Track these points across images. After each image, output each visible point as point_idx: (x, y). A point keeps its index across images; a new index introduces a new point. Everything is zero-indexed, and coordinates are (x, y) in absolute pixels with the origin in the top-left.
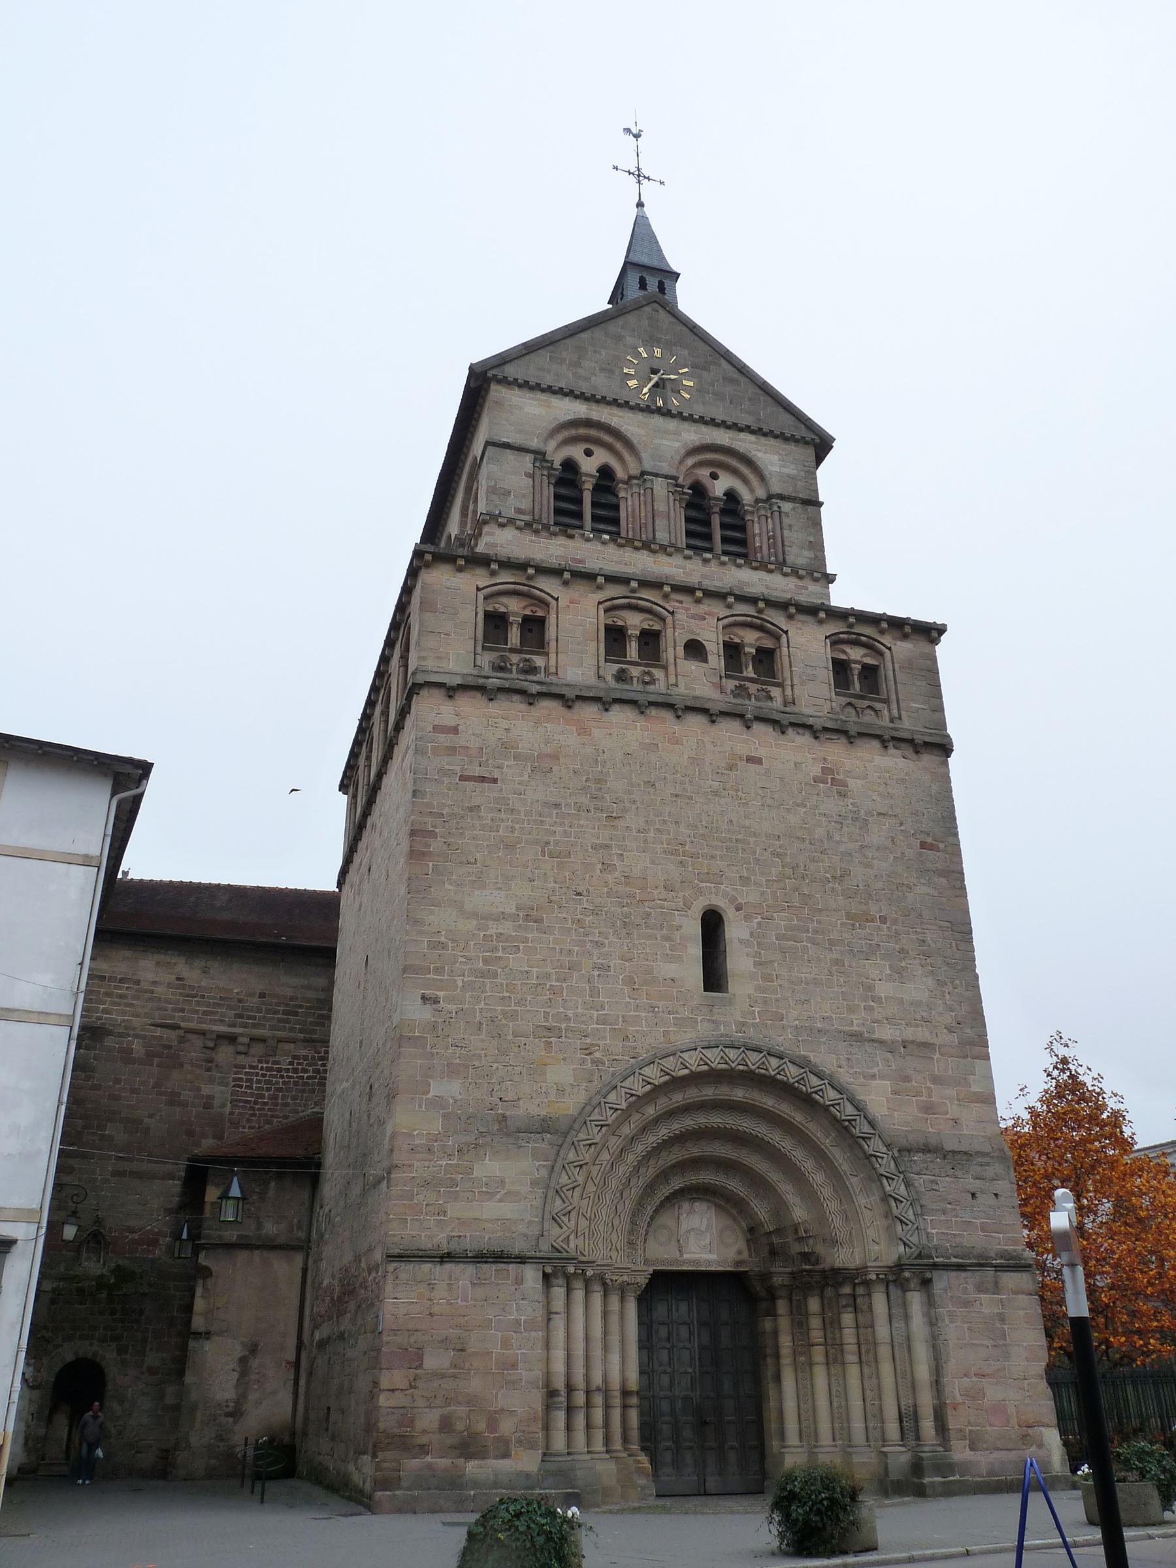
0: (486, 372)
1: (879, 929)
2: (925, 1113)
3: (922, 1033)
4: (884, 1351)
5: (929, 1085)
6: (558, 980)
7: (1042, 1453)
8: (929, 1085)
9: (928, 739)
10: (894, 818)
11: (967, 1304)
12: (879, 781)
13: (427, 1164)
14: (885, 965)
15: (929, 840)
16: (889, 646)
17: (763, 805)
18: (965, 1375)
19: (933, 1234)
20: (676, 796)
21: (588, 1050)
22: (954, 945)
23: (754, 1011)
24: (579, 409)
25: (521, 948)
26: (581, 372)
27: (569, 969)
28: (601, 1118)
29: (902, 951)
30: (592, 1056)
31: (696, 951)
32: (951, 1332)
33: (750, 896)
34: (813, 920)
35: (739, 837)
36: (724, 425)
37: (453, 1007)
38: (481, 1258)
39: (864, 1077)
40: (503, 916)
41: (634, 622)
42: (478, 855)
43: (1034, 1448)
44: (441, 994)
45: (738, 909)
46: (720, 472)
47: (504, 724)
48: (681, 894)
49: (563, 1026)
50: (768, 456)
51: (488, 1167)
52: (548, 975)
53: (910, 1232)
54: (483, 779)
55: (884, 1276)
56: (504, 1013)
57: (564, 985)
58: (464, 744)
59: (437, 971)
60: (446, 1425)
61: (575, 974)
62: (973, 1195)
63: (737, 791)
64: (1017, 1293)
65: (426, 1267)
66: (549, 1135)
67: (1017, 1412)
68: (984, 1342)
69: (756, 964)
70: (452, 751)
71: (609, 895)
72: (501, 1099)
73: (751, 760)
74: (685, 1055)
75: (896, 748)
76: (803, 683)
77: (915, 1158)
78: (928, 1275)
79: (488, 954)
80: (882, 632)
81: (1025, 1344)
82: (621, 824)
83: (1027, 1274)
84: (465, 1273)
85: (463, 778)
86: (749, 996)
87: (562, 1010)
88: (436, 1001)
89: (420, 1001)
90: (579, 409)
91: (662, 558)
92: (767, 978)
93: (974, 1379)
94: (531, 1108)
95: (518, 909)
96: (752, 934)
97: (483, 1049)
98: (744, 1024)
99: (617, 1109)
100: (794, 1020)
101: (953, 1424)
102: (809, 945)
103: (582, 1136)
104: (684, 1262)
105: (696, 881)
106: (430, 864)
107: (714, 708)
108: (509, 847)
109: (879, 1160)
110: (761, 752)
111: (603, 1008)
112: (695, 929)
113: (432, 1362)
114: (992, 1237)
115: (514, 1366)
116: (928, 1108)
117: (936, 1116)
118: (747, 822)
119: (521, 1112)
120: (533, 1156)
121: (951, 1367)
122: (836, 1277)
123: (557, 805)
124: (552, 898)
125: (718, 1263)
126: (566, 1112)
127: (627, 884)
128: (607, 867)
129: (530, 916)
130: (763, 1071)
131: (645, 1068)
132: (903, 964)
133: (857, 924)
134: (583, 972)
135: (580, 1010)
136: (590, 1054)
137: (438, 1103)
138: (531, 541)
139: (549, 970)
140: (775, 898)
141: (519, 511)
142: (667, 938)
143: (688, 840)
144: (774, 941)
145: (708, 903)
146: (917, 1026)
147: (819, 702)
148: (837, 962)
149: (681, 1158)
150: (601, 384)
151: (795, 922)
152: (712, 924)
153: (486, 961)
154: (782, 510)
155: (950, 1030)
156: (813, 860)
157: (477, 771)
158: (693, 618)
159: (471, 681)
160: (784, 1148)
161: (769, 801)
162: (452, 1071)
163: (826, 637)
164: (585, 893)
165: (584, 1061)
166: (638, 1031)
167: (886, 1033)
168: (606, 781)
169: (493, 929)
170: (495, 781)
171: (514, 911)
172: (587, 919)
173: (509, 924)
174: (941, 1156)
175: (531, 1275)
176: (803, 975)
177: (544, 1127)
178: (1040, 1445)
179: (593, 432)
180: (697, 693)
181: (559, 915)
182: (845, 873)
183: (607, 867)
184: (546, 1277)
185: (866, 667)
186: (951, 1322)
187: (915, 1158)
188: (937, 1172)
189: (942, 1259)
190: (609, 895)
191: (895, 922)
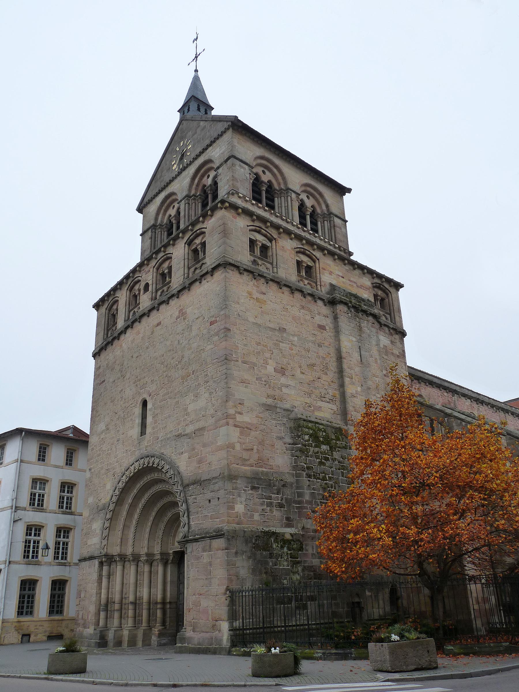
15: (214, 319)
33: (152, 388)
68: (203, 577)
73: (159, 324)
80: (203, 222)
93: (197, 596)
161: (162, 340)
167: (190, 429)
174: (199, 484)
188: (196, 493)
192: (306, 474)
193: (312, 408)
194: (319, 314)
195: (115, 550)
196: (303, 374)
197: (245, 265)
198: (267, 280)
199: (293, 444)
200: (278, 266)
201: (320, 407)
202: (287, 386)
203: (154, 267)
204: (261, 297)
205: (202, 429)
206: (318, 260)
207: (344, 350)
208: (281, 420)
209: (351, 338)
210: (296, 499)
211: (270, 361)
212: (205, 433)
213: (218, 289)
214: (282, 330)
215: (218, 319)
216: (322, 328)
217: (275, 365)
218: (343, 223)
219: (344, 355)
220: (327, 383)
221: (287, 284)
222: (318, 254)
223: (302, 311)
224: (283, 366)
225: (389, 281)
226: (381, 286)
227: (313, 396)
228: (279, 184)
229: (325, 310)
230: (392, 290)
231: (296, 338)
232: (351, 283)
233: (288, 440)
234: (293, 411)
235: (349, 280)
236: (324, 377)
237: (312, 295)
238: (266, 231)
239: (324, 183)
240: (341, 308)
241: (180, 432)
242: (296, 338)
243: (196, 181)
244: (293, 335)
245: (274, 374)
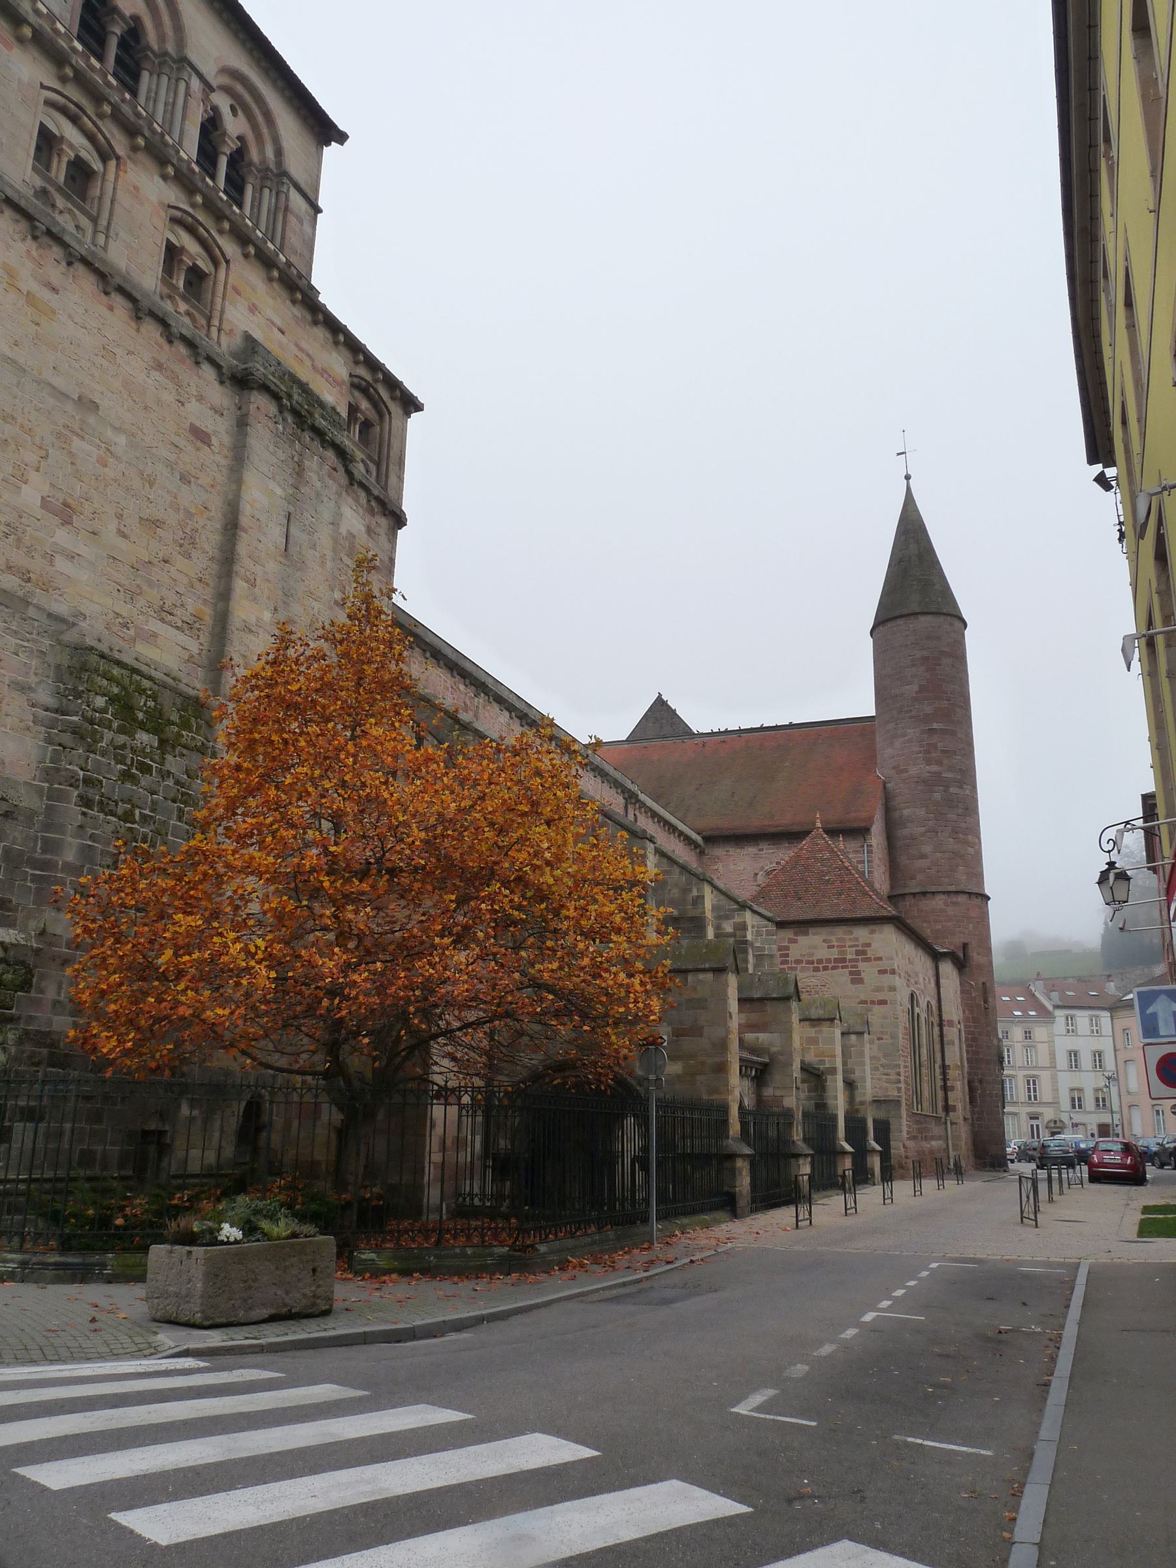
192: (81, 797)
193: (132, 632)
194: (200, 398)
196: (125, 536)
197: (12, 187)
198: (70, 254)
199: (56, 711)
200: (112, 233)
201: (155, 635)
202: (71, 557)
204: (45, 295)
206: (227, 262)
207: (246, 509)
208: (34, 641)
209: (272, 485)
210: (37, 855)
211: (33, 476)
214: (88, 405)
216: (200, 436)
217: (46, 490)
218: (311, 212)
219: (244, 521)
220: (186, 581)
221: (128, 287)
222: (230, 247)
223: (155, 374)
224: (70, 501)
225: (393, 384)
226: (371, 389)
227: (141, 602)
228: (162, 38)
229: (219, 395)
230: (395, 409)
231: (122, 440)
232: (299, 354)
233: (45, 696)
234: (74, 624)
235: (297, 345)
236: (180, 562)
237: (191, 344)
238: (94, 123)
239: (281, 91)
240: (260, 403)
242: (122, 440)
244: (118, 430)
245: (38, 512)
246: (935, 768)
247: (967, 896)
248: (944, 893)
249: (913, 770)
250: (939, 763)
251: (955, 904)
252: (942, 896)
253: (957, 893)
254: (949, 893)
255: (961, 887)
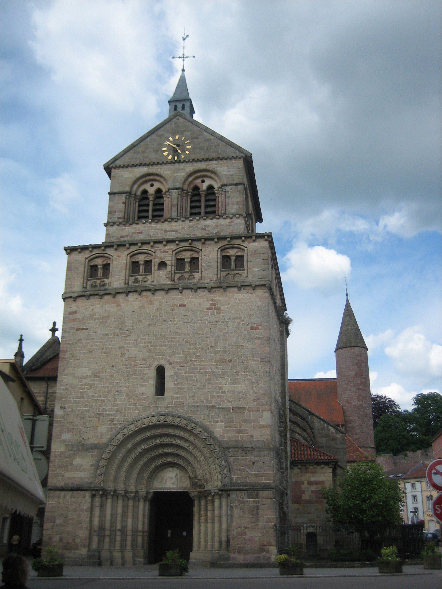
0: (109, 166)
1: (228, 364)
2: (238, 434)
3: (242, 404)
4: (216, 519)
5: (241, 423)
6: (103, 397)
7: (268, 555)
8: (241, 423)
9: (257, 284)
10: (240, 319)
11: (243, 503)
12: (235, 304)
13: (60, 460)
14: (229, 379)
15: (255, 326)
16: (246, 246)
17: (184, 323)
18: (239, 527)
19: (234, 478)
20: (149, 324)
21: (112, 421)
22: (260, 367)
23: (172, 402)
24: (144, 170)
25: (92, 387)
26: (146, 155)
27: (107, 393)
28: (114, 443)
29: (237, 372)
30: (113, 423)
31: (152, 382)
32: (236, 512)
33: (175, 359)
34: (200, 365)
35: (174, 336)
36: (203, 160)
37: (70, 409)
38: (72, 489)
39: (214, 422)
40: (86, 377)
41: (141, 258)
42: (80, 356)
43: (264, 553)
44: (66, 405)
45: (170, 364)
46: (205, 179)
47: (92, 307)
48: (148, 362)
49: (104, 413)
50: (222, 168)
51: (77, 461)
52: (100, 396)
53: (224, 478)
54: (84, 329)
55: (217, 493)
56: (86, 410)
57: (105, 399)
58: (78, 317)
59: (66, 398)
60: (61, 540)
61: (110, 395)
62: (254, 463)
63: (174, 318)
64: (265, 498)
65: (58, 492)
66: (97, 450)
67: (259, 540)
69: (175, 384)
70: (74, 320)
71: (123, 365)
72: (83, 438)
73: (181, 305)
74: (145, 420)
75: (244, 289)
76: (206, 270)
77: (230, 451)
78: (228, 493)
79: (82, 390)
80: (243, 241)
81: (266, 517)
82: (128, 338)
83: (271, 491)
84: (69, 494)
85: (78, 330)
86: (171, 396)
87: (104, 408)
88: (65, 408)
89: (60, 409)
90: (144, 170)
91: (173, 224)
92: (179, 389)
93: (243, 529)
94: (92, 441)
95: (92, 374)
96: (175, 373)
97: (78, 423)
98: (168, 407)
99: (120, 440)
100: (188, 403)
101: (232, 544)
102: (197, 375)
103: (107, 450)
104: (166, 488)
105: (155, 356)
106: (65, 361)
107: (166, 288)
108: (91, 352)
109: (215, 452)
110: (186, 301)
111: (118, 406)
112: (152, 373)
113: (58, 521)
114: (259, 478)
115: (81, 522)
116: (239, 432)
117: (242, 435)
118: (177, 330)
119: (89, 443)
120: (91, 457)
121: (234, 524)
122: (208, 493)
123: (107, 335)
124: (104, 369)
125: (177, 488)
126: (104, 442)
127: (129, 360)
128: (123, 355)
129: (96, 376)
130: (173, 423)
131: (131, 426)
132: (237, 377)
133: (219, 364)
134: (112, 394)
135: (110, 407)
136: (113, 422)
137: (64, 441)
138: (122, 229)
139: (101, 394)
140: (185, 357)
141: (119, 218)
142: (142, 379)
143: (153, 341)
144: (183, 374)
145: (158, 363)
146: (239, 401)
147: (211, 276)
148: (207, 380)
149: (157, 454)
150: (153, 157)
151: (193, 367)
152: (161, 372)
153: (81, 393)
154: (227, 190)
155: (254, 401)
156: (203, 341)
157: (82, 326)
158: (163, 253)
159: (80, 294)
160: (189, 449)
162: (69, 430)
163: (219, 248)
164: (115, 365)
165: (110, 424)
166: (129, 413)
168: (125, 323)
169: (84, 381)
170: (87, 329)
171: (90, 374)
172: (115, 374)
173: (89, 379)
175: (88, 494)
176: (193, 386)
177: (96, 447)
178: (268, 552)
179: (152, 177)
180: (161, 283)
181: (106, 374)
182: (216, 344)
183: (123, 355)
184: (93, 496)
185: (237, 257)
186: (236, 509)
187: (230, 451)
189: (235, 487)
190: (123, 365)
191: (235, 361)
195: (110, 486)
203: (173, 251)
205: (244, 408)
212: (245, 412)
213: (260, 303)
215: (260, 327)
241: (213, 404)
243: (191, 179)
246: (361, 403)
247: (371, 448)
248: (364, 447)
249: (353, 403)
250: (362, 401)
251: (368, 451)
252: (364, 448)
253: (368, 447)
254: (366, 447)
255: (369, 445)
